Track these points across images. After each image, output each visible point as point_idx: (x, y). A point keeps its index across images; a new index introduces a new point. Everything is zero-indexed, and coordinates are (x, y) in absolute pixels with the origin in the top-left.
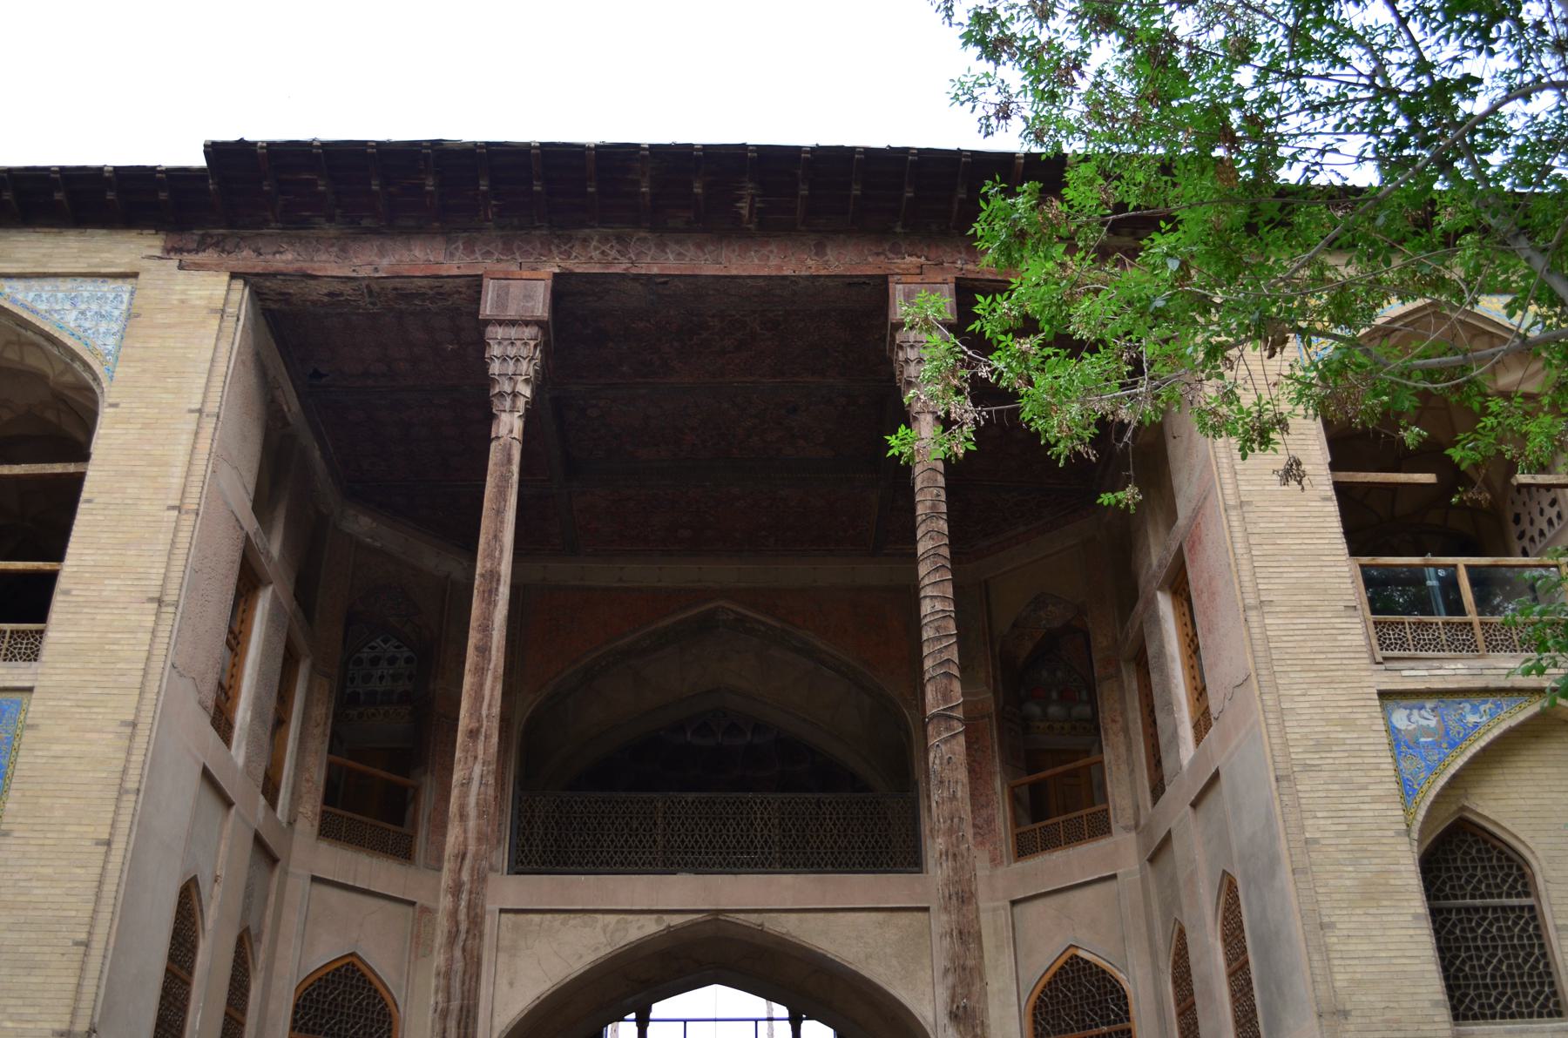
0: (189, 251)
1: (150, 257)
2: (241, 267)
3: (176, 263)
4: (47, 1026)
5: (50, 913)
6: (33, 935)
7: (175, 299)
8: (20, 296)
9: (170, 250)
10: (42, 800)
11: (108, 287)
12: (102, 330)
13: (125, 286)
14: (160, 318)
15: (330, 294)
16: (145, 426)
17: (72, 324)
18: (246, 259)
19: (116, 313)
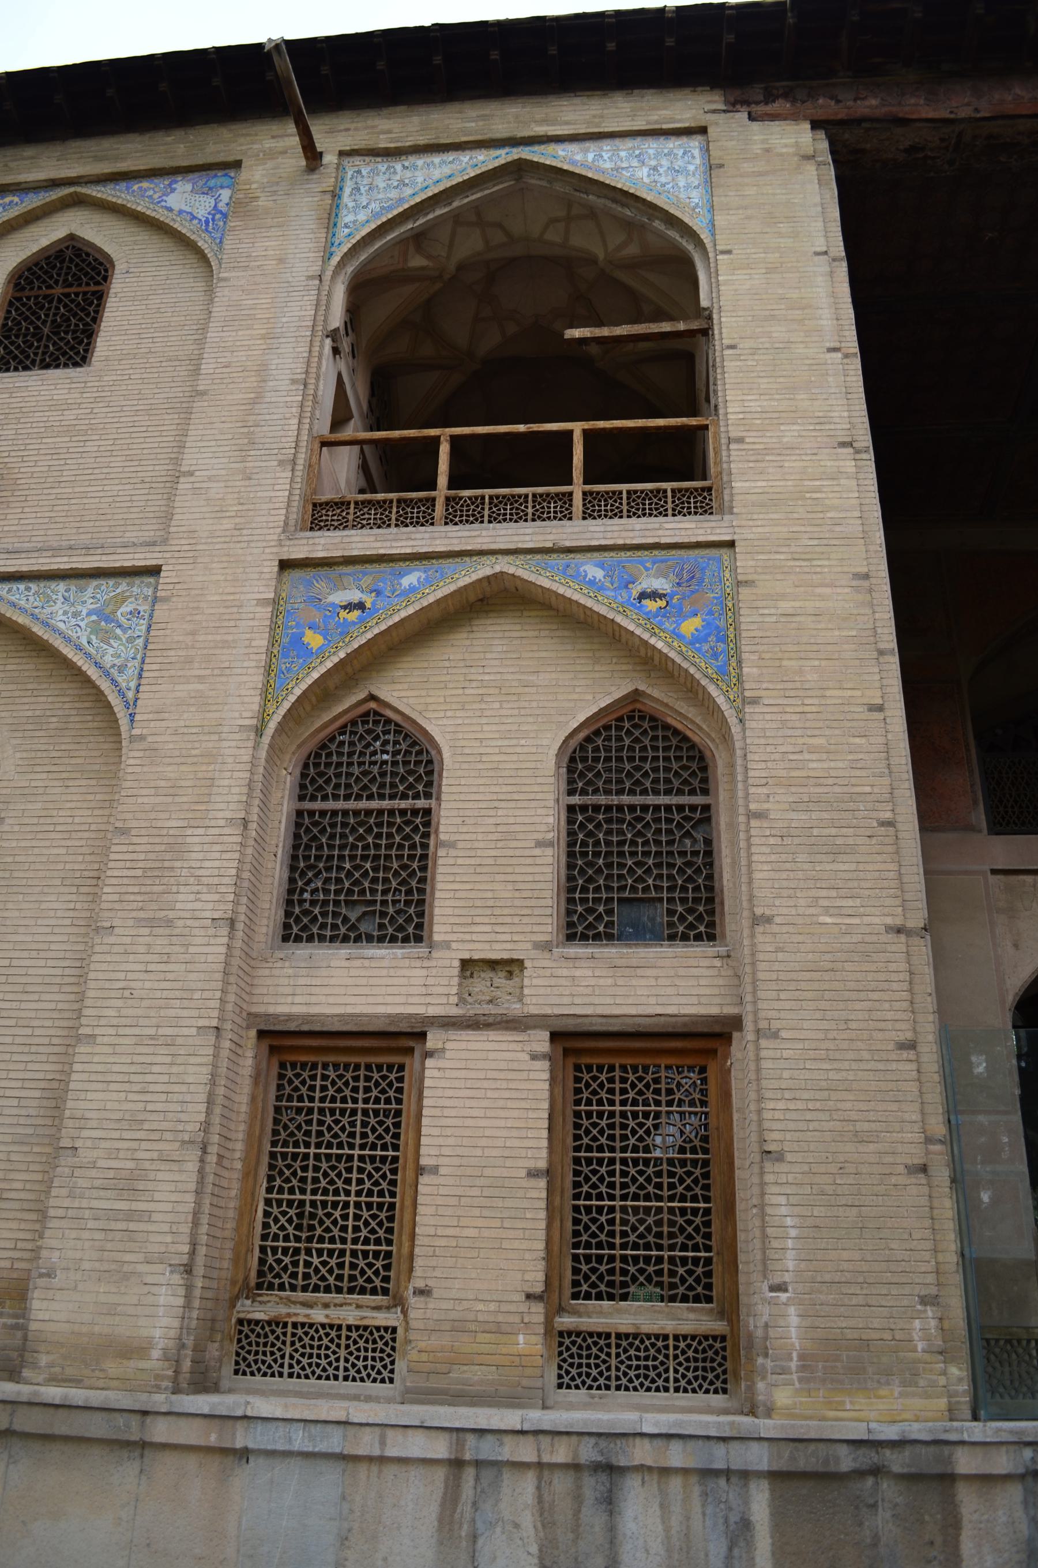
0: (757, 103)
1: (714, 111)
2: (820, 114)
3: (746, 115)
4: (876, 920)
5: (837, 789)
6: (825, 815)
7: (757, 149)
8: (578, 157)
9: (733, 105)
10: (785, 663)
11: (673, 144)
12: (682, 184)
13: (694, 144)
14: (747, 167)
15: (912, 149)
16: (770, 271)
17: (646, 180)
18: (825, 107)
19: (691, 168)
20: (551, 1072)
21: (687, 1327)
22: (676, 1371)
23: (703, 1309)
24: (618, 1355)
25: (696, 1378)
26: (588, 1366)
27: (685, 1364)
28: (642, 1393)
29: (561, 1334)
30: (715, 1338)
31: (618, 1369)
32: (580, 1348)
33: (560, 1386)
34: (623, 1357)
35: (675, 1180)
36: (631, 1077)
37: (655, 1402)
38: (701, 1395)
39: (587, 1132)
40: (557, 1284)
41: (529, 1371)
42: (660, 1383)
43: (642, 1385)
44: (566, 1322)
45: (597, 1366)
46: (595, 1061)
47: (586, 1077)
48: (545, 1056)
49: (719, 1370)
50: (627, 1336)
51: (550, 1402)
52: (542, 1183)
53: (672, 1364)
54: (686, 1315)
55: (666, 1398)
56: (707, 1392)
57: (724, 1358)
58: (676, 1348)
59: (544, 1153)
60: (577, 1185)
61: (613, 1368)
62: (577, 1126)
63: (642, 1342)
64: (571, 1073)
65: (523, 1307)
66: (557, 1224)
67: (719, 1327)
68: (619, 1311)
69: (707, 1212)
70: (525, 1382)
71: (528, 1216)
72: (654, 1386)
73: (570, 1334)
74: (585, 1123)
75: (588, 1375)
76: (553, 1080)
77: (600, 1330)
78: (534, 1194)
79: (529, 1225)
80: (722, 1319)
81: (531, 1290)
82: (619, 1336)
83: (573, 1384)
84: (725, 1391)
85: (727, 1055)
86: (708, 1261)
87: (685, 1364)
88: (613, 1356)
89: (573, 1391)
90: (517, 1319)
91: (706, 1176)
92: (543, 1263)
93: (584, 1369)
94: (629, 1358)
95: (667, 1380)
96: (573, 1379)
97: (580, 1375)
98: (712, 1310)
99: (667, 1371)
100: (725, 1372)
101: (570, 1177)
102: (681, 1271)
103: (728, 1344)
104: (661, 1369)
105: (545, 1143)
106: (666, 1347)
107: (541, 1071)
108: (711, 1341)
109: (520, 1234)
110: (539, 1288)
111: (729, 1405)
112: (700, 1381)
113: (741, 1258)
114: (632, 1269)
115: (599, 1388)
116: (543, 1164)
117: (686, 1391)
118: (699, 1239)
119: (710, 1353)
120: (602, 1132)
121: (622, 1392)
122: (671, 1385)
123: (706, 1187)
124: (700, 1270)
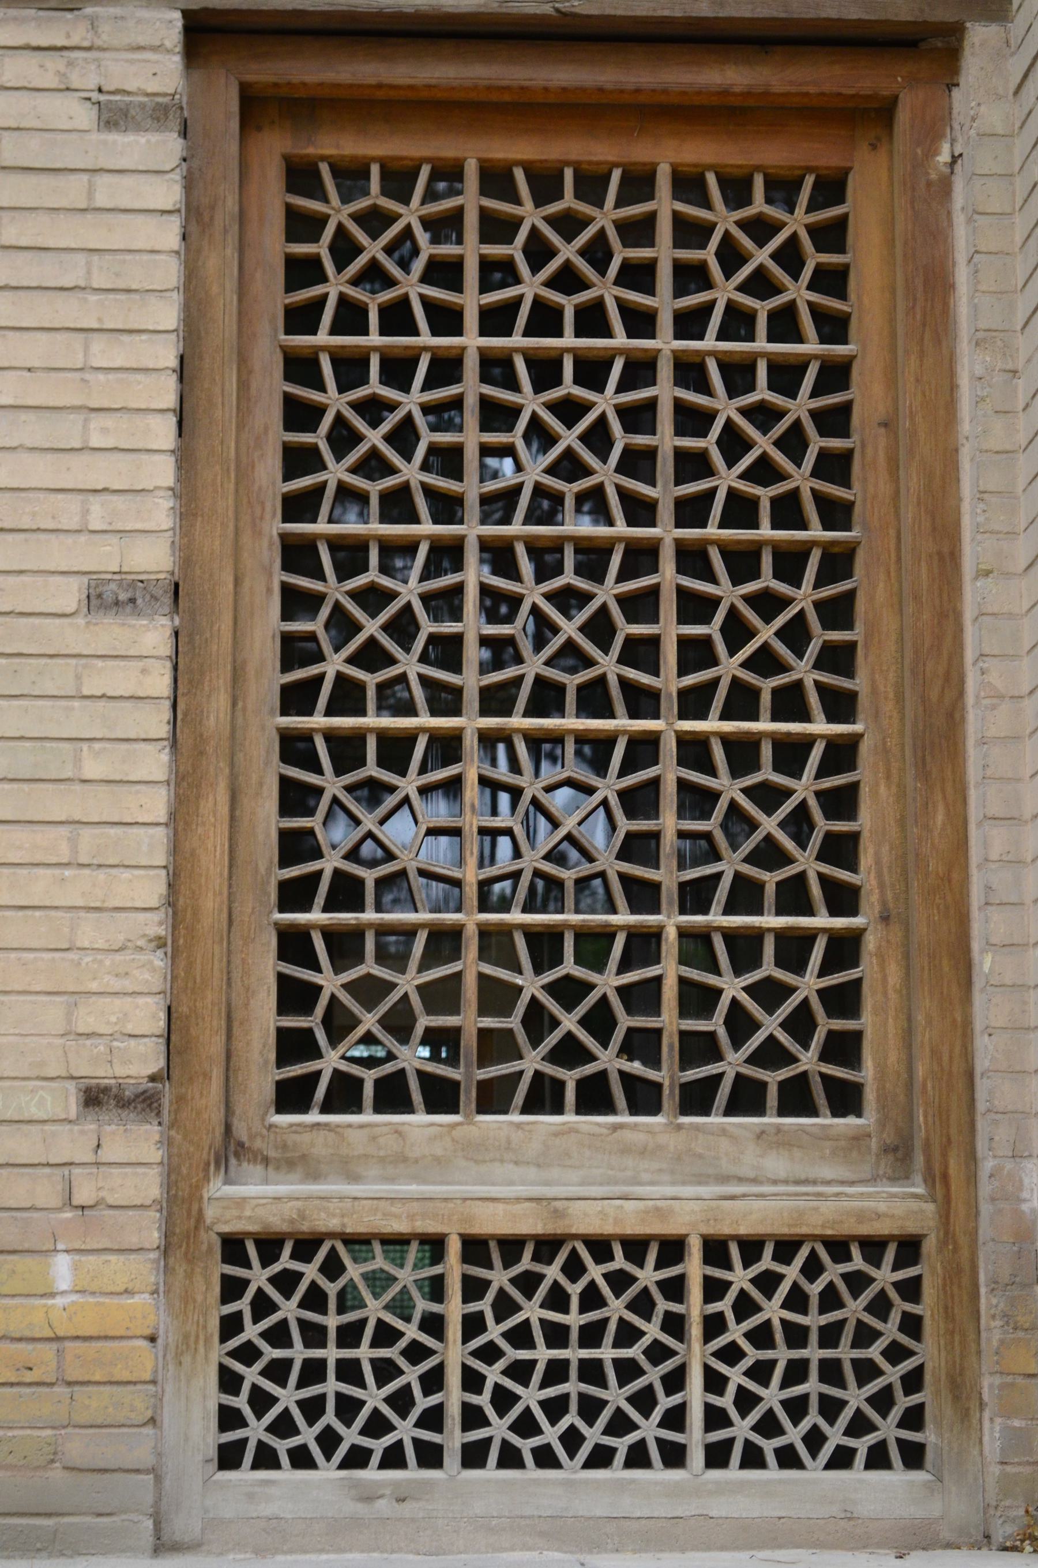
20: (189, 184)
21: (758, 1213)
22: (714, 1382)
23: (825, 1135)
24: (473, 1325)
25: (796, 1408)
26: (349, 1371)
27: (753, 1355)
28: (572, 1470)
29: (233, 1248)
30: (873, 1248)
31: (472, 1381)
32: (315, 1299)
33: (229, 1457)
34: (494, 1332)
35: (713, 629)
36: (531, 215)
37: (629, 1506)
38: (814, 1474)
39: (344, 438)
40: (214, 1045)
41: (95, 1403)
42: (649, 1429)
43: (572, 1440)
44: (253, 1198)
45: (385, 1371)
46: (375, 146)
47: (338, 212)
48: (160, 113)
49: (893, 1374)
50: (511, 1247)
51: (184, 1524)
52: (154, 635)
53: (696, 1354)
54: (752, 1159)
55: (675, 1491)
56: (842, 1459)
57: (912, 1325)
58: (714, 1289)
59: (161, 514)
60: (296, 651)
61: (454, 1378)
62: (299, 415)
63: (574, 1269)
64: (273, 198)
65: (73, 1143)
66: (216, 802)
67: (892, 1205)
68: (474, 1151)
69: (841, 755)
70: (78, 1447)
71: (92, 769)
72: (622, 1444)
73: (269, 1247)
74: (335, 401)
75: (347, 1408)
76: (195, 215)
77: (399, 1226)
78: (120, 680)
79: (98, 805)
80: (902, 1172)
81: (103, 1073)
82: (475, 1249)
83: (282, 1446)
84: (914, 1456)
85: (935, 126)
86: (844, 950)
87: (753, 1355)
88: (454, 1329)
89: (287, 1475)
90: (45, 1191)
91: (838, 612)
92: (158, 961)
93: (332, 1386)
94: (521, 1336)
95: (675, 1418)
96: (284, 1426)
97: (313, 1409)
98: (858, 1139)
99: (675, 1381)
100: (913, 1381)
101: (268, 623)
102: (732, 987)
103: (929, 1269)
104: (653, 1375)
105: (163, 472)
106: (675, 1289)
107: (148, 174)
108: (857, 1262)
109: (56, 844)
110: (140, 1062)
111: (934, 1508)
112: (813, 1418)
113: (986, 926)
114: (531, 984)
115: (394, 1458)
116: (154, 558)
117: (753, 1459)
118: (806, 862)
119: (854, 1309)
120: (403, 437)
121: (491, 1473)
122: (695, 1437)
123: (839, 659)
124: (809, 984)
